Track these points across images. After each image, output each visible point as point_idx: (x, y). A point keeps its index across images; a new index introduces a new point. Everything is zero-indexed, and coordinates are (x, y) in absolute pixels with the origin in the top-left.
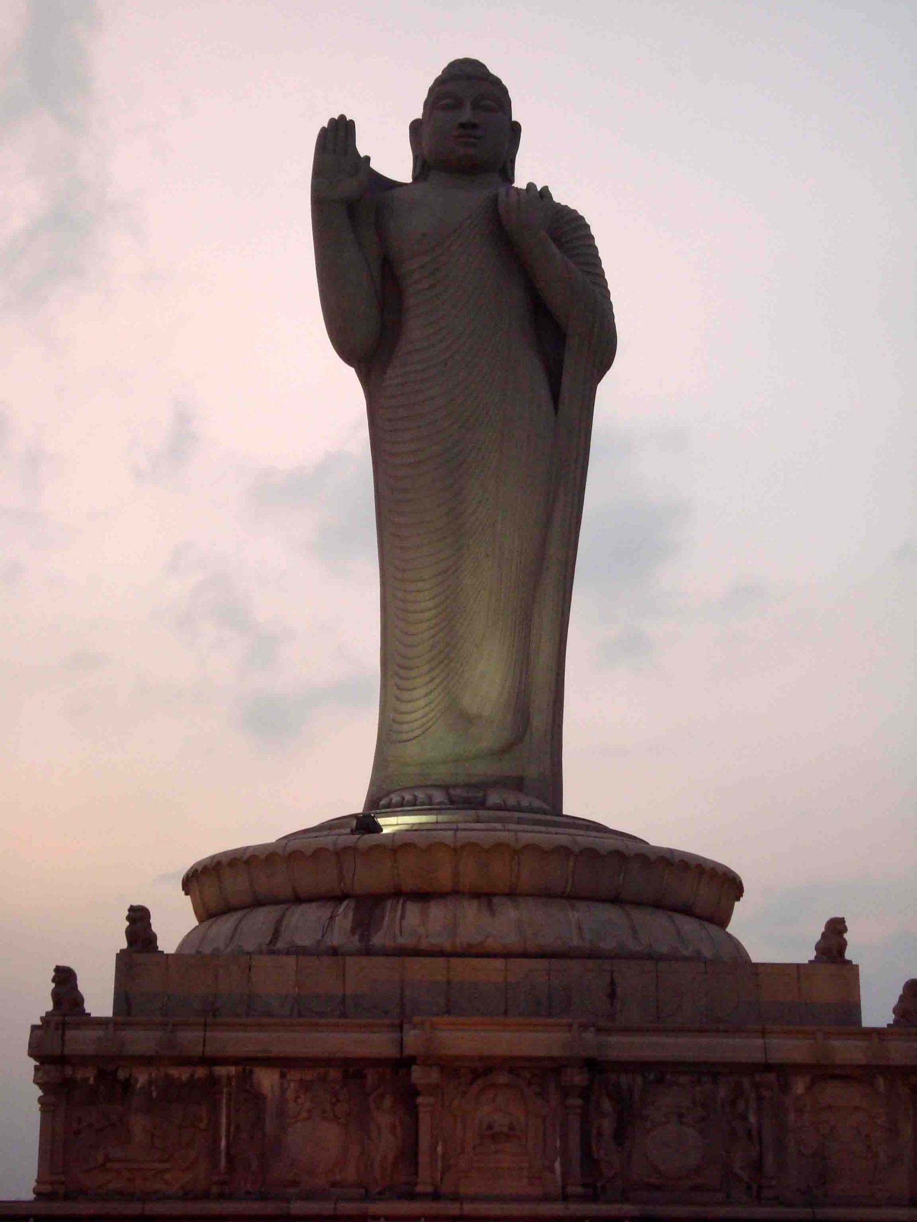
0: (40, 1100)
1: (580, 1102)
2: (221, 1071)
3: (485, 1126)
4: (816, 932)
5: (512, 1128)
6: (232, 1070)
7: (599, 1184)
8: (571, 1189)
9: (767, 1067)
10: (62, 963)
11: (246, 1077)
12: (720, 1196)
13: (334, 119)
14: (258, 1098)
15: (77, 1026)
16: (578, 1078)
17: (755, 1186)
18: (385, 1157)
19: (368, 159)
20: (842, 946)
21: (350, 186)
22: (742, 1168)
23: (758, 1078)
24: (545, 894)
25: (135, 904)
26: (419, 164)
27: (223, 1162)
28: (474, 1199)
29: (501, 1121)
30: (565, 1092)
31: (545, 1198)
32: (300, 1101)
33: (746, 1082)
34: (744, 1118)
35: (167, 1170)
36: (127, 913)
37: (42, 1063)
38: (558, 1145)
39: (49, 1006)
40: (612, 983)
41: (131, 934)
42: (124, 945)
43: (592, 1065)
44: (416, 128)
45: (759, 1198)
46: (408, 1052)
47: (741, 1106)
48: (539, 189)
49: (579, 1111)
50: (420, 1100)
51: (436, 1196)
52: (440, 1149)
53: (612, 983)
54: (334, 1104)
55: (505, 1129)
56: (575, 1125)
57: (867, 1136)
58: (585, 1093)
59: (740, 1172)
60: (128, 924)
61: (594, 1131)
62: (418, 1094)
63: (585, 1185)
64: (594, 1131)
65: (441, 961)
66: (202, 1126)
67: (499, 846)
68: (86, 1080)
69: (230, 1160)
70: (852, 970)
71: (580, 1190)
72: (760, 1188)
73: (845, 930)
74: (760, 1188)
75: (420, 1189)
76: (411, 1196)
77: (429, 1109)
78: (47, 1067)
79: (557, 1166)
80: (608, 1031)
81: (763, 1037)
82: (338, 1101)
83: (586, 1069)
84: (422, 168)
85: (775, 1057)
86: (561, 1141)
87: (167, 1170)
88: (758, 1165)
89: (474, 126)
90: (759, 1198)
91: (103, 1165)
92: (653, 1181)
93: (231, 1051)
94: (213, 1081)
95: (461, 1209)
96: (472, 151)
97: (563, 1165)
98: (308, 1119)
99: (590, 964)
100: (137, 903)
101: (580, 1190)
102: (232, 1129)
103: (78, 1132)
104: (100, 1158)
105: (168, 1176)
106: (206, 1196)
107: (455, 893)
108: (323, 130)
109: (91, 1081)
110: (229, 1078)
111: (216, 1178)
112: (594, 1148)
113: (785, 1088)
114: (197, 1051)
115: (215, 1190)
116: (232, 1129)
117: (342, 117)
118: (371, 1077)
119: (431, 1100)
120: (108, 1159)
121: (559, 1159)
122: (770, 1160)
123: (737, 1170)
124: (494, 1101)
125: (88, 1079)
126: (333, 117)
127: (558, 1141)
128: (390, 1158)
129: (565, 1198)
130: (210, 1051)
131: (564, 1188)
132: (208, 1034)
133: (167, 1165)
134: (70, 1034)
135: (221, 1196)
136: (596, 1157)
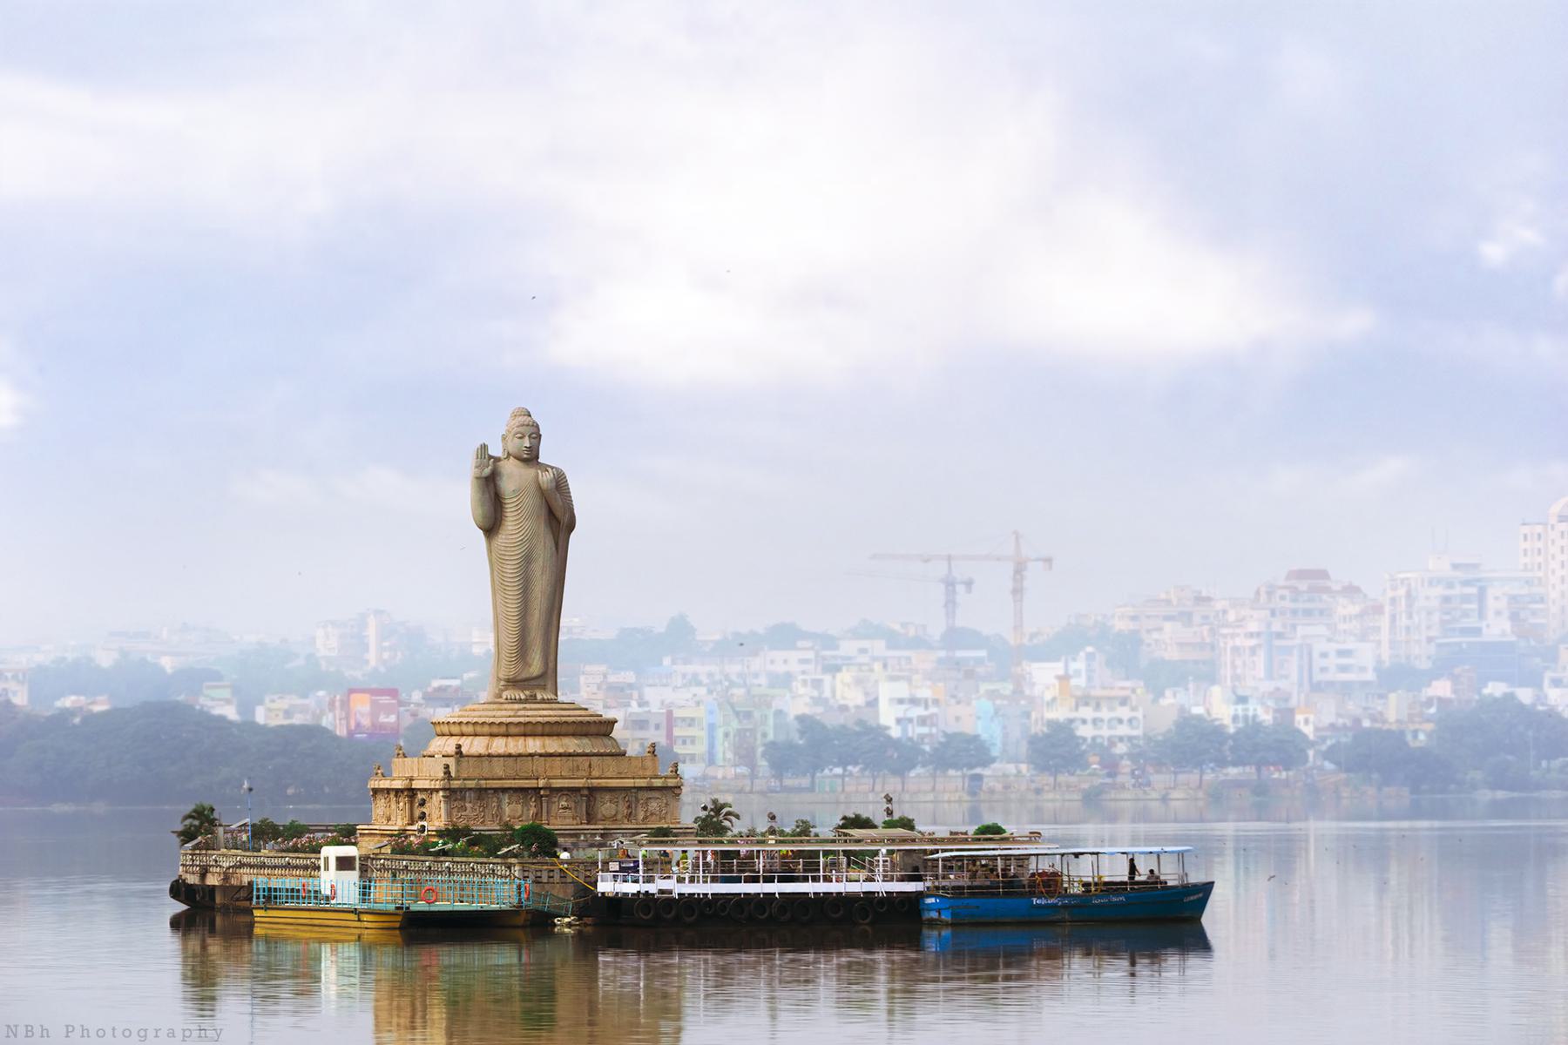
9: (635, 788)
16: (586, 792)
65: (543, 758)
107: (542, 735)
129: (581, 824)
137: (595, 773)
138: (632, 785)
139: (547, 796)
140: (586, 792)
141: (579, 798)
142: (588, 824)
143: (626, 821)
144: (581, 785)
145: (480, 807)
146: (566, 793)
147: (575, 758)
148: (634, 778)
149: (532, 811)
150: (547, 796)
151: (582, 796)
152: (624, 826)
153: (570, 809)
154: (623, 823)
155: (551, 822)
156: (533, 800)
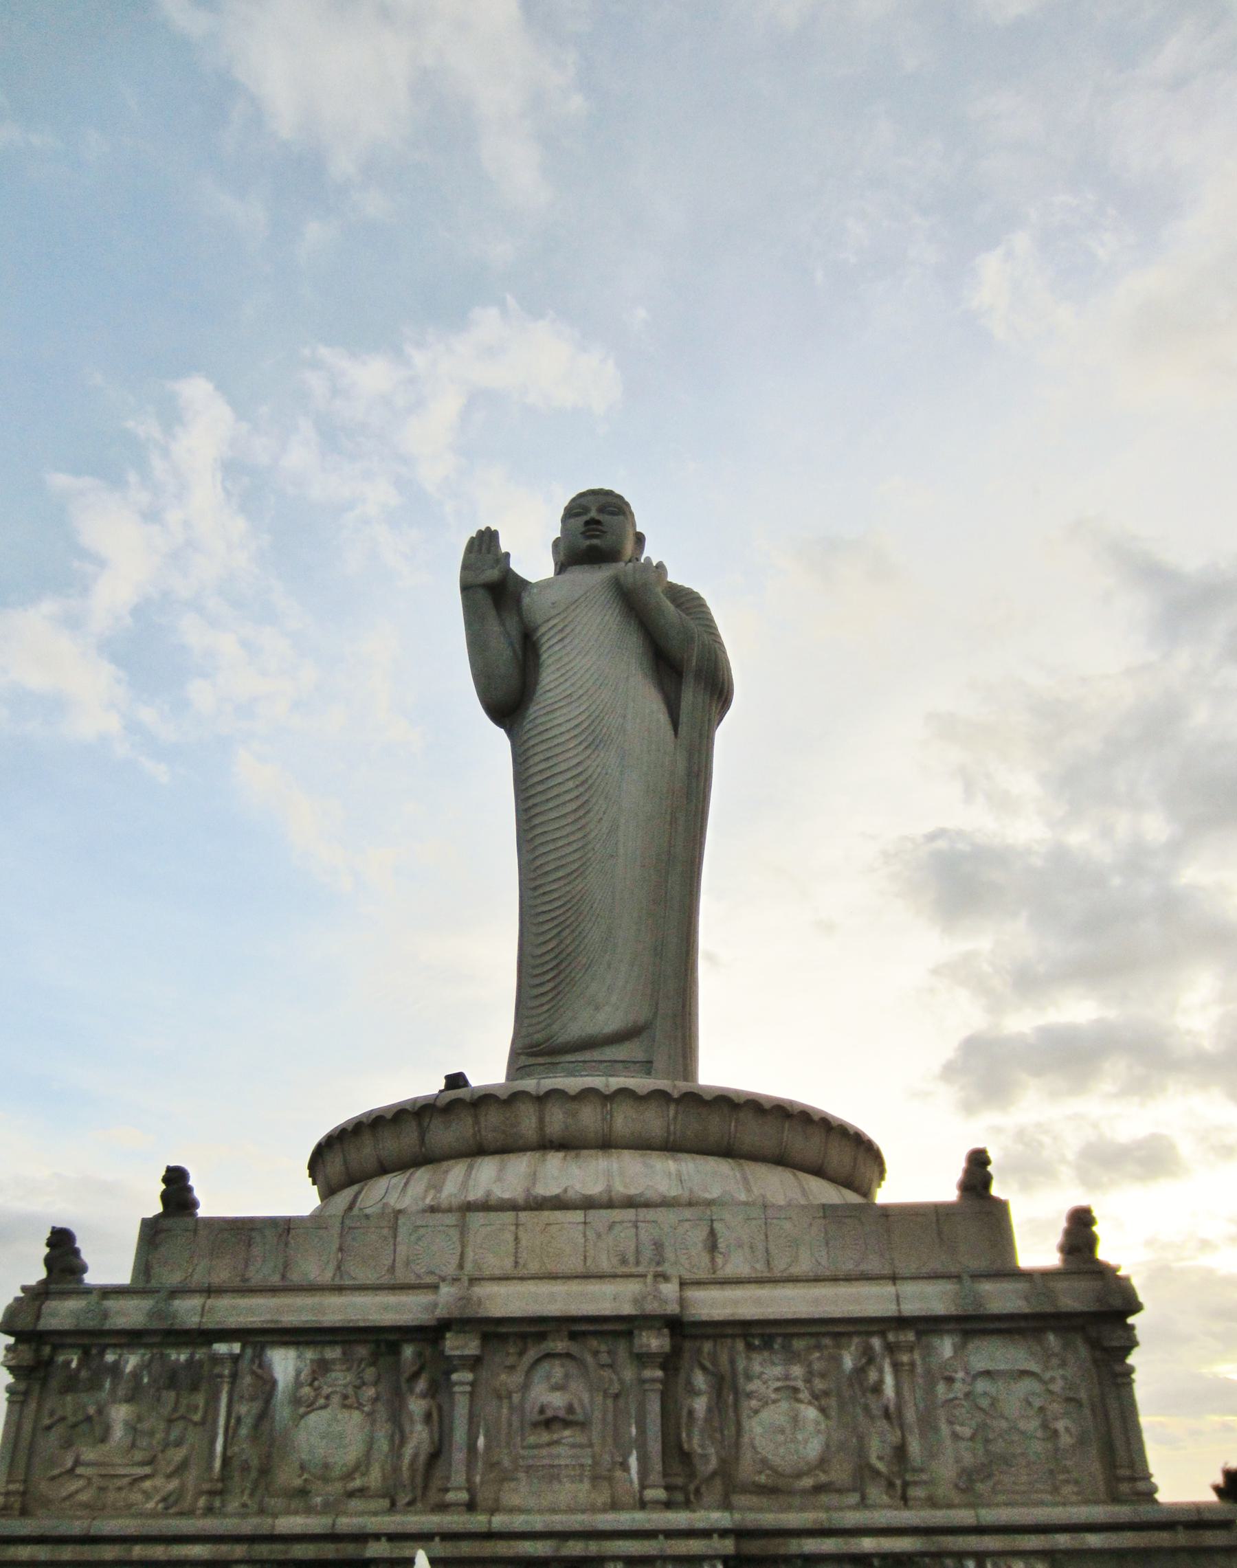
0: (10, 1389)
1: (659, 1373)
2: (221, 1348)
3: (536, 1409)
4: (956, 1169)
5: (570, 1409)
6: (236, 1348)
7: (692, 1487)
8: (650, 1494)
9: (902, 1322)
10: (59, 1225)
11: (259, 1357)
12: (854, 1498)
13: (480, 530)
14: (267, 1384)
15: (64, 1294)
16: (655, 1342)
17: (898, 1482)
18: (415, 1456)
19: (507, 555)
20: (986, 1180)
21: (492, 574)
22: (880, 1458)
23: (891, 1337)
24: (642, 1145)
25: (172, 1164)
26: (558, 567)
27: (218, 1464)
28: (521, 1510)
29: (557, 1400)
30: (642, 1359)
31: (614, 1506)
32: (316, 1383)
33: (876, 1342)
34: (877, 1389)
35: (146, 1477)
36: (163, 1173)
37: (17, 1342)
38: (634, 1430)
39: (41, 1273)
40: (712, 1233)
41: (165, 1197)
42: (158, 1208)
43: (677, 1326)
44: (556, 544)
45: (905, 1499)
46: (441, 1312)
47: (873, 1376)
48: (654, 564)
49: (659, 1386)
50: (455, 1377)
51: (471, 1506)
52: (481, 1442)
53: (712, 1233)
54: (357, 1388)
55: (562, 1414)
56: (654, 1407)
57: (1041, 1409)
58: (670, 1362)
59: (880, 1466)
60: (163, 1187)
61: (685, 1413)
62: (455, 1370)
63: (667, 1488)
64: (685, 1413)
65: (509, 1216)
66: (197, 1417)
67: (587, 1094)
68: (69, 1363)
69: (226, 1461)
70: (1000, 1208)
71: (660, 1494)
72: (906, 1485)
73: (987, 1162)
74: (906, 1485)
75: (451, 1496)
76: (443, 1507)
77: (468, 1388)
78: (20, 1347)
79: (633, 1461)
80: (699, 1283)
81: (895, 1284)
82: (364, 1384)
83: (666, 1331)
84: (561, 568)
85: (911, 1308)
86: (637, 1428)
87: (146, 1477)
88: (900, 1452)
89: (598, 522)
90: (905, 1499)
91: (72, 1470)
92: (762, 1479)
93: (233, 1322)
94: (216, 1360)
95: (490, 1522)
96: (595, 541)
97: (638, 1459)
98: (324, 1407)
99: (687, 1213)
100: (174, 1163)
101: (660, 1494)
102: (233, 1421)
103: (49, 1428)
104: (69, 1464)
105: (147, 1484)
106: (189, 1513)
108: (472, 538)
109: (74, 1365)
110: (236, 1359)
111: (206, 1486)
112: (684, 1435)
113: (928, 1351)
114: (193, 1321)
115: (202, 1502)
116: (233, 1421)
117: (488, 529)
118: (408, 1351)
119: (469, 1376)
120: (77, 1463)
121: (634, 1452)
122: (914, 1447)
123: (874, 1460)
124: (548, 1377)
125: (72, 1361)
126: (480, 528)
127: (634, 1426)
128: (422, 1458)
129: (643, 1505)
130: (210, 1323)
131: (641, 1492)
132: (209, 1302)
133: (147, 1470)
134: (52, 1305)
135: (209, 1511)
136: (686, 1446)
137: (737, 1265)
138: (889, 1309)
139: (475, 1363)
140: (655, 1342)
141: (628, 1374)
142: (668, 1505)
143: (875, 1493)
144: (627, 1309)
145: (170, 1421)
146: (560, 1346)
147: (643, 1213)
148: (894, 1278)
149: (419, 1436)
150: (475, 1363)
151: (642, 1359)
152: (852, 1518)
153: (583, 1425)
154: (863, 1504)
155: (484, 1496)
156: (421, 1385)
